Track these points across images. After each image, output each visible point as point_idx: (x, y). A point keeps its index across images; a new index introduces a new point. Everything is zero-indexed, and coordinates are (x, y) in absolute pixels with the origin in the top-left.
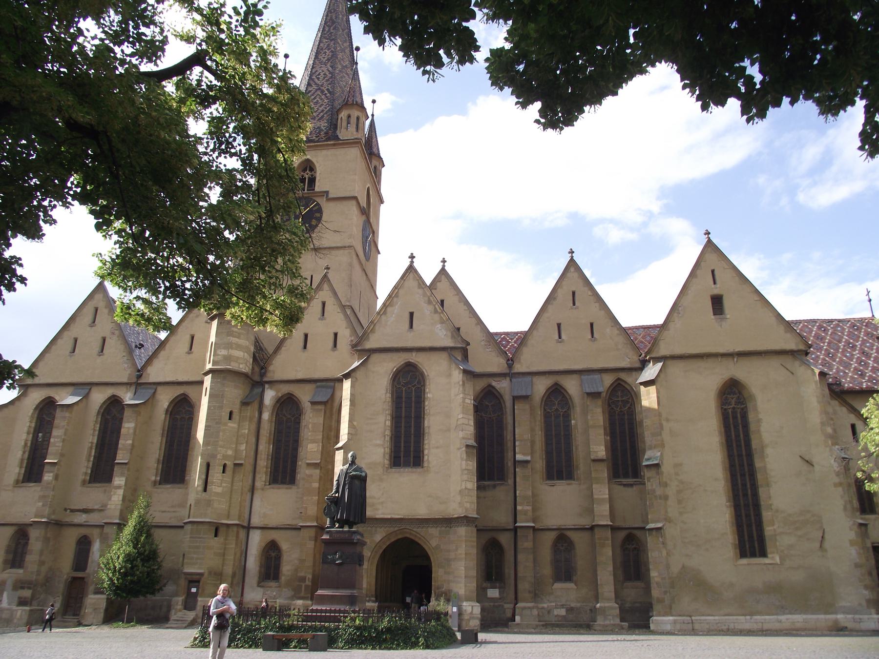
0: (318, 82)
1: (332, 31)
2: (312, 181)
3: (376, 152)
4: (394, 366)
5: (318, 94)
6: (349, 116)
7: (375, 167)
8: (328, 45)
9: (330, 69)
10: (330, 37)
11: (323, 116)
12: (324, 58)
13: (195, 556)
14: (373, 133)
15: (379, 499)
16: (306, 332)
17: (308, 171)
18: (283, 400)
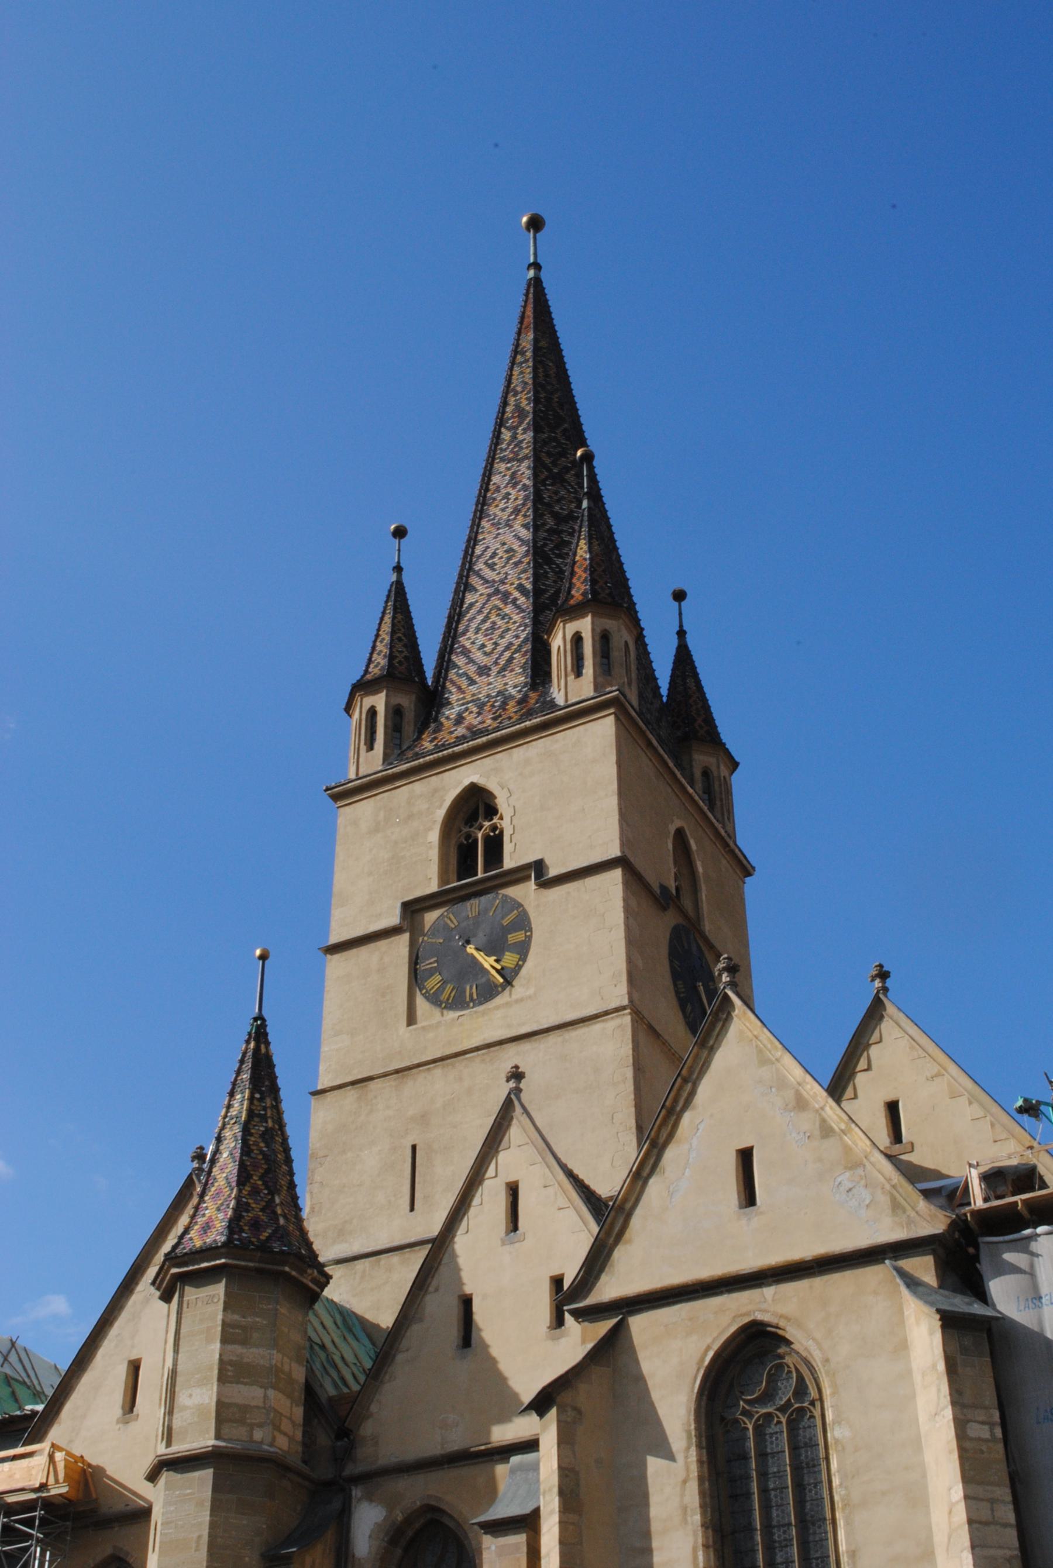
1: (520, 437)
2: (495, 845)
6: (578, 639)
7: (706, 773)
10: (516, 454)
11: (510, 660)
12: (503, 510)
14: (690, 682)
17: (480, 820)
18: (410, 1533)
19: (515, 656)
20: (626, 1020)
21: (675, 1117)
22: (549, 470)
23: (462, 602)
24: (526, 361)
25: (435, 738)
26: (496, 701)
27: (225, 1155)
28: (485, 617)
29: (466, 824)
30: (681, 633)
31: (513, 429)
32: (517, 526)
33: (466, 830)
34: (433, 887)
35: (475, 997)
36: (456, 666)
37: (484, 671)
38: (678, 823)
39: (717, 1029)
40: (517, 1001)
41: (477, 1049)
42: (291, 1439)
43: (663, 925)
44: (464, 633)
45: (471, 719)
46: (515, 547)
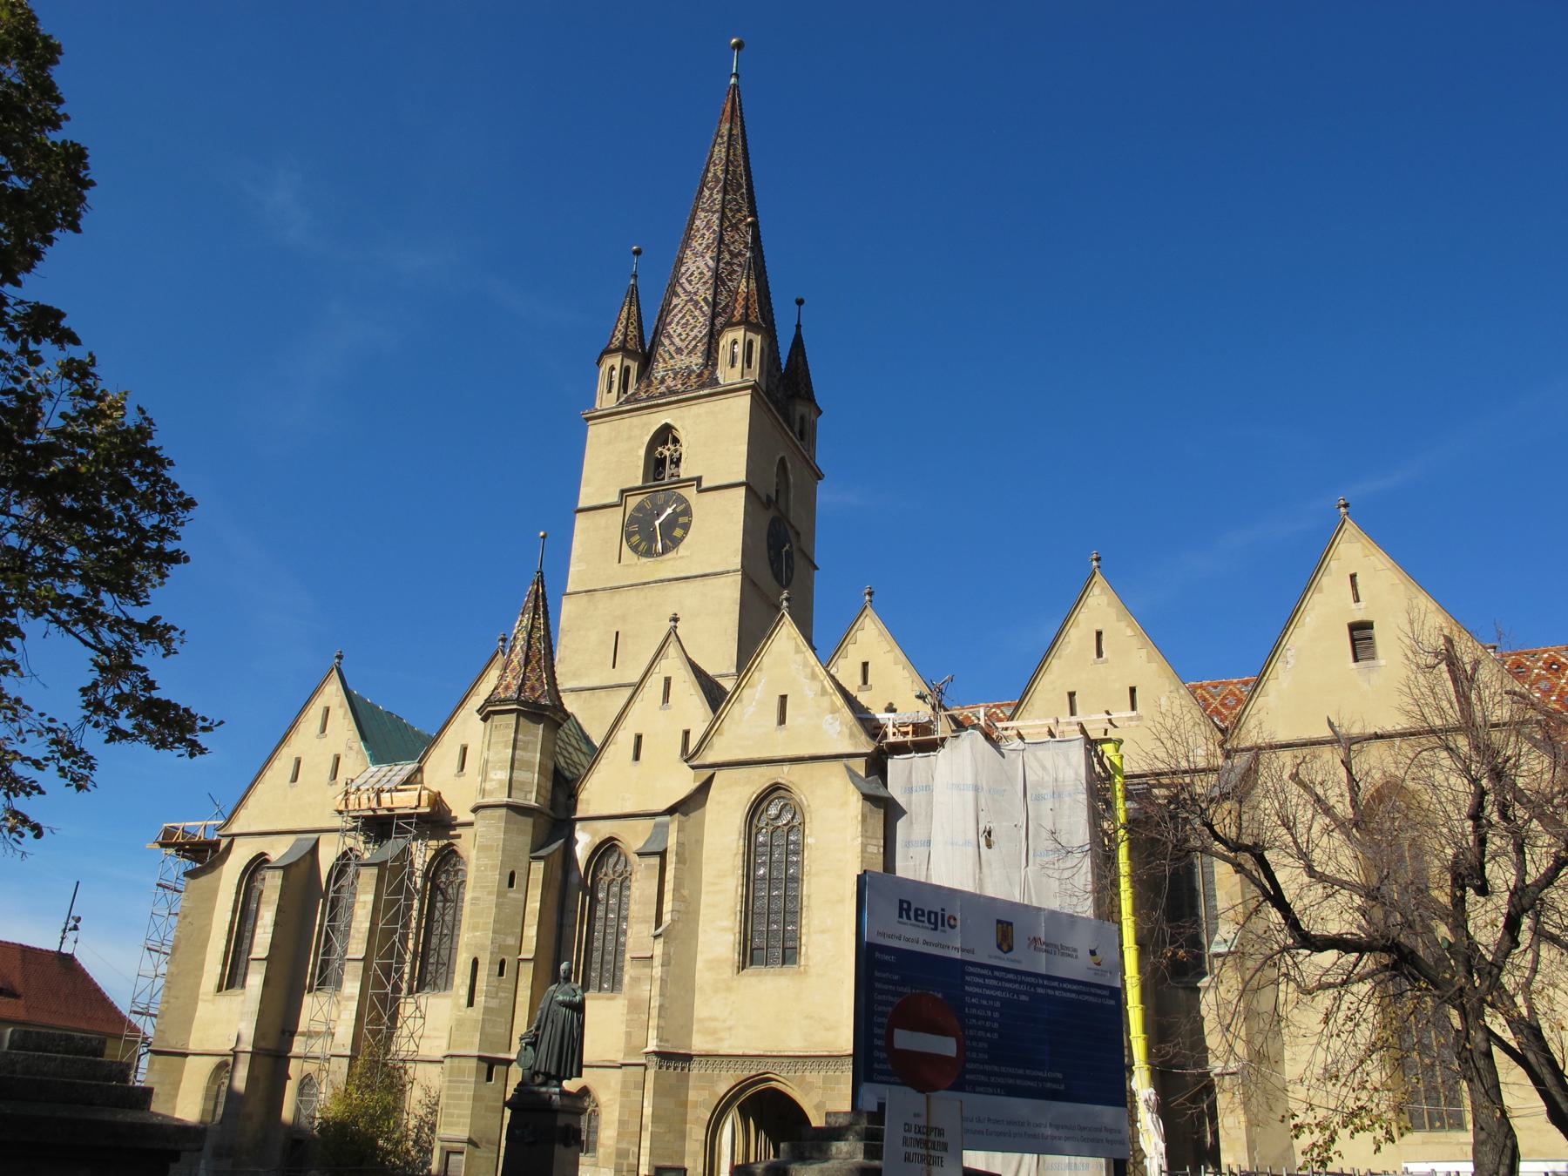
0: (689, 288)
1: (715, 197)
4: (751, 792)
5: (689, 309)
7: (802, 418)
8: (707, 223)
9: (711, 263)
11: (696, 346)
13: (456, 1111)
15: (724, 1021)
16: (639, 732)
20: (738, 577)
22: (730, 221)
23: (671, 303)
24: (723, 143)
25: (647, 391)
27: (518, 648)
30: (798, 326)
31: (711, 189)
32: (707, 258)
34: (639, 483)
36: (663, 345)
37: (679, 351)
38: (781, 454)
40: (681, 558)
41: (656, 582)
42: (545, 798)
43: (765, 518)
44: (670, 324)
45: (669, 382)
46: (705, 272)
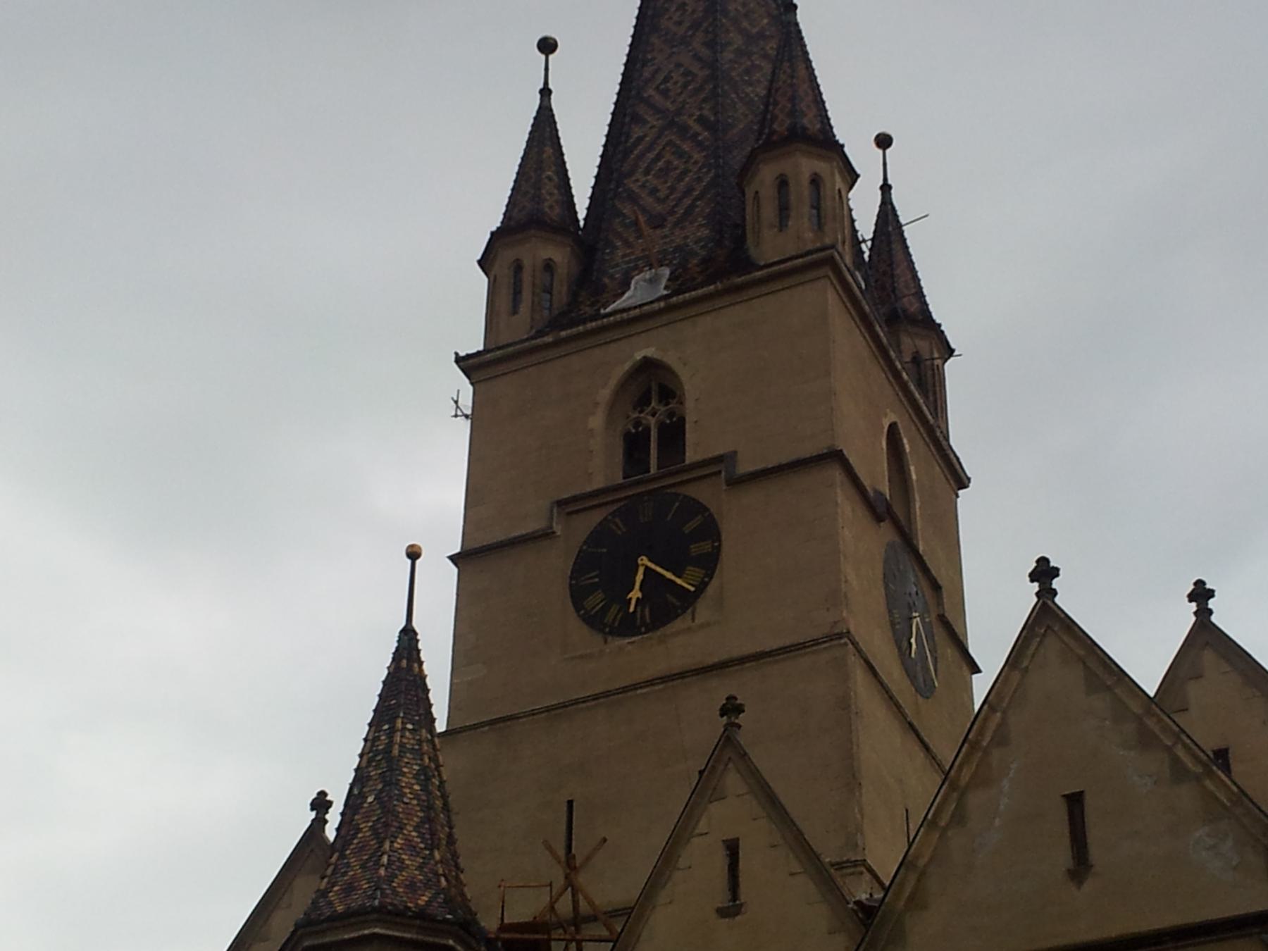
2: (674, 433)
3: (914, 307)
5: (670, 143)
6: (782, 183)
9: (705, 52)
11: (692, 206)
12: (680, 23)
19: (699, 203)
21: (980, 754)
23: (628, 136)
26: (675, 258)
28: (658, 155)
29: (635, 409)
33: (636, 415)
35: (648, 621)
37: (657, 222)
39: (1033, 648)
40: (702, 626)
41: (650, 683)
44: (631, 173)
46: (695, 69)
